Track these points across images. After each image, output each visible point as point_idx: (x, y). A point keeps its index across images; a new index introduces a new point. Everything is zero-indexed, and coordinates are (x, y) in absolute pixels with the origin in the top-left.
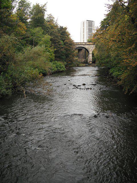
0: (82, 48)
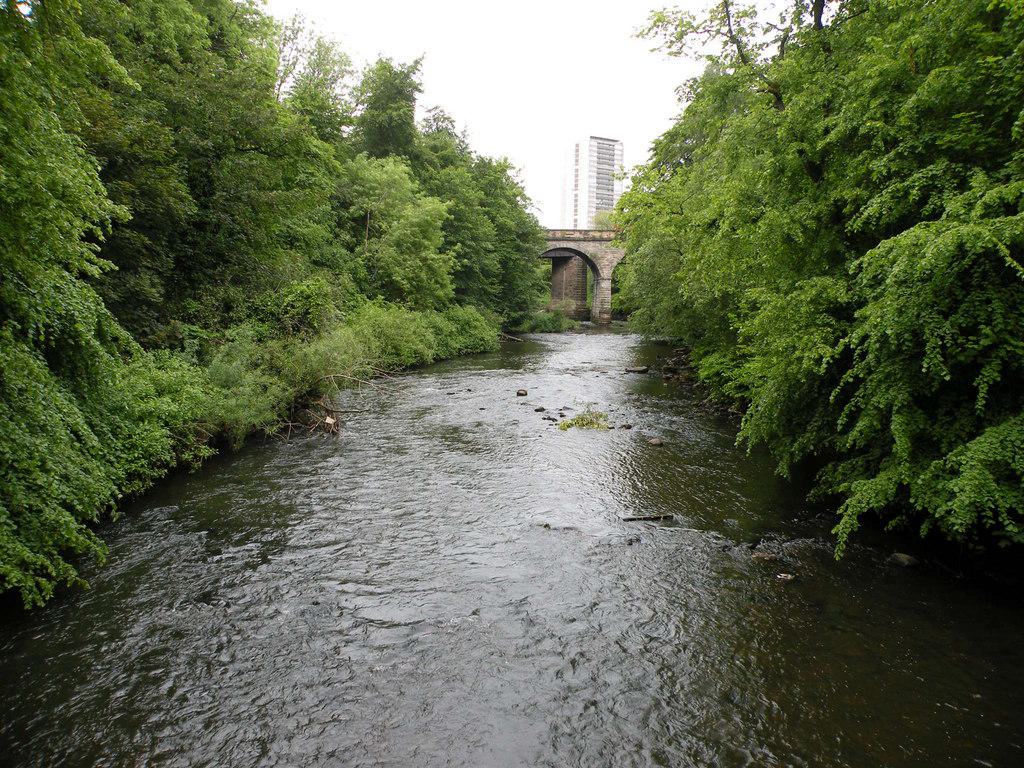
0: (572, 254)
